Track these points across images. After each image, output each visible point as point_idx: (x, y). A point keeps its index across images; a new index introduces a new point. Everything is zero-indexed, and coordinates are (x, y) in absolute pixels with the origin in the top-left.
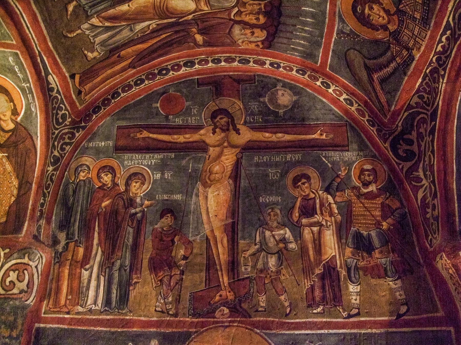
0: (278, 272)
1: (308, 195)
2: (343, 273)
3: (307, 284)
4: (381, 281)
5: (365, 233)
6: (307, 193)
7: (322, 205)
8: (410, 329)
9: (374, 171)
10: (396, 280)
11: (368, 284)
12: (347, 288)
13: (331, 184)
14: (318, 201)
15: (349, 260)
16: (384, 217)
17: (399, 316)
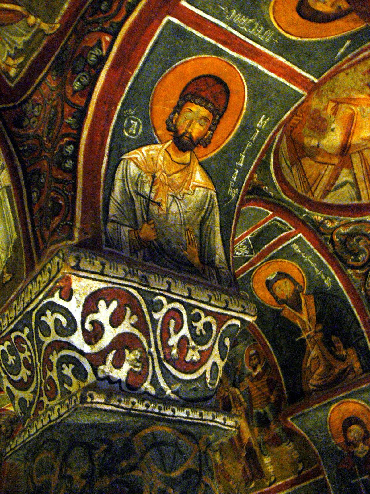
0: (223, 464)
1: (224, 395)
2: (257, 449)
3: (240, 467)
4: (280, 449)
5: (261, 411)
6: (223, 393)
7: (234, 399)
8: (308, 483)
9: (257, 353)
10: (289, 443)
11: (275, 454)
12: (263, 460)
13: (235, 378)
14: (231, 397)
15: (259, 438)
16: (271, 392)
17: (299, 473)
